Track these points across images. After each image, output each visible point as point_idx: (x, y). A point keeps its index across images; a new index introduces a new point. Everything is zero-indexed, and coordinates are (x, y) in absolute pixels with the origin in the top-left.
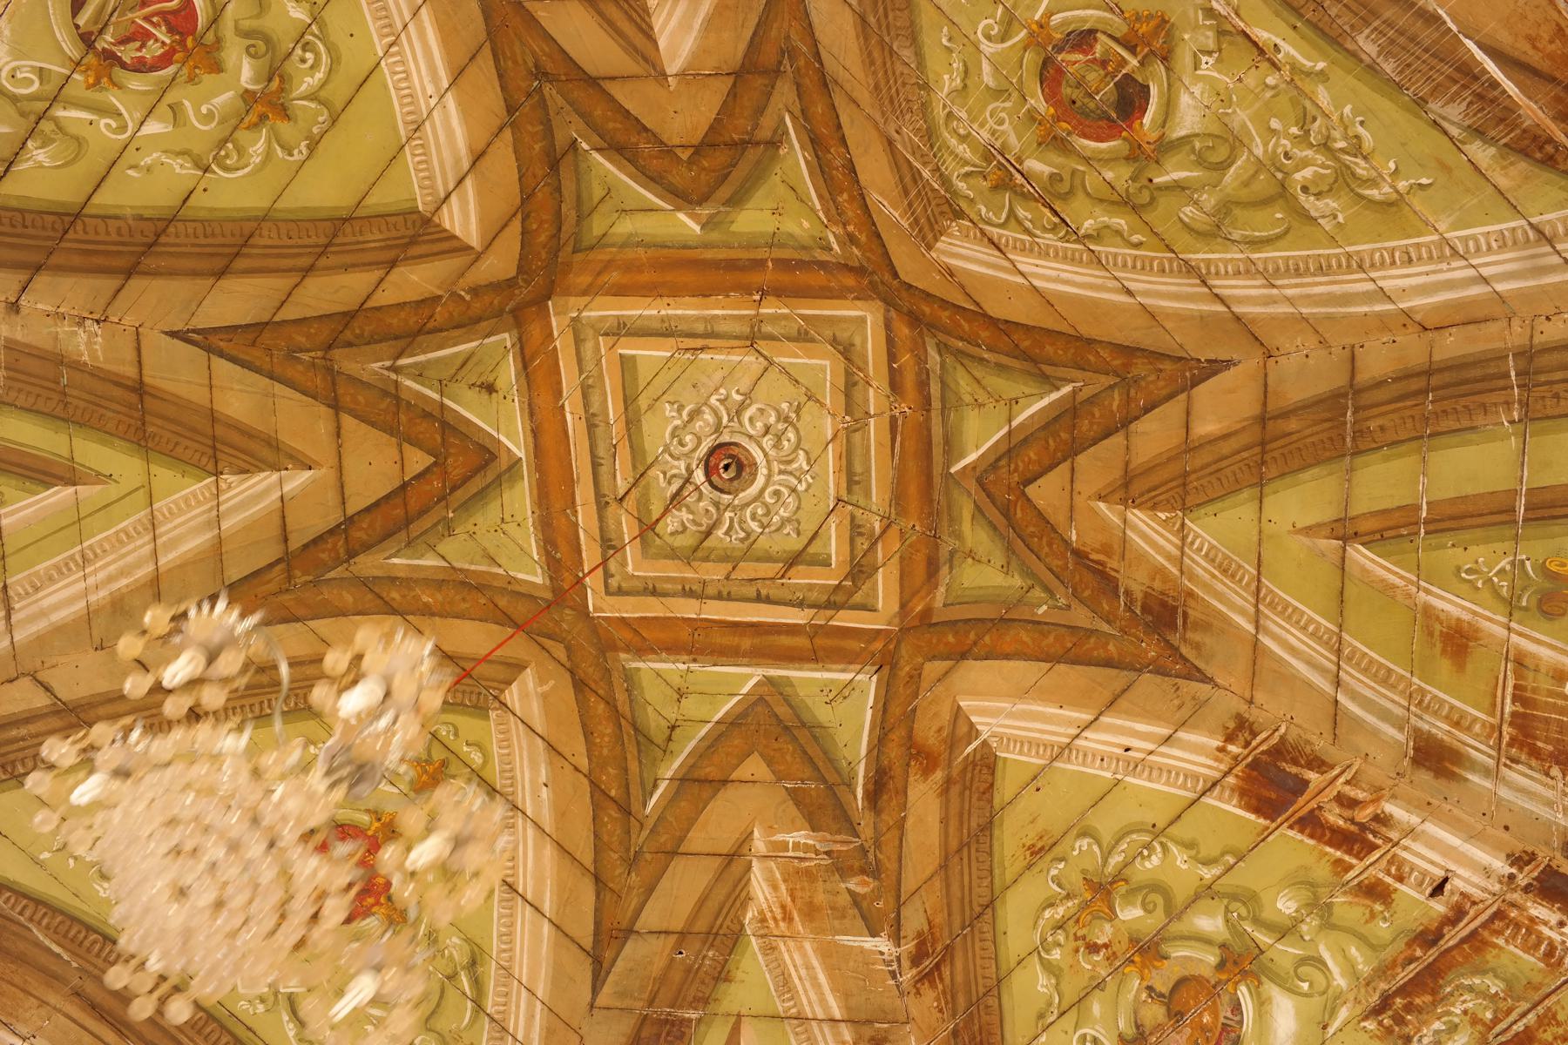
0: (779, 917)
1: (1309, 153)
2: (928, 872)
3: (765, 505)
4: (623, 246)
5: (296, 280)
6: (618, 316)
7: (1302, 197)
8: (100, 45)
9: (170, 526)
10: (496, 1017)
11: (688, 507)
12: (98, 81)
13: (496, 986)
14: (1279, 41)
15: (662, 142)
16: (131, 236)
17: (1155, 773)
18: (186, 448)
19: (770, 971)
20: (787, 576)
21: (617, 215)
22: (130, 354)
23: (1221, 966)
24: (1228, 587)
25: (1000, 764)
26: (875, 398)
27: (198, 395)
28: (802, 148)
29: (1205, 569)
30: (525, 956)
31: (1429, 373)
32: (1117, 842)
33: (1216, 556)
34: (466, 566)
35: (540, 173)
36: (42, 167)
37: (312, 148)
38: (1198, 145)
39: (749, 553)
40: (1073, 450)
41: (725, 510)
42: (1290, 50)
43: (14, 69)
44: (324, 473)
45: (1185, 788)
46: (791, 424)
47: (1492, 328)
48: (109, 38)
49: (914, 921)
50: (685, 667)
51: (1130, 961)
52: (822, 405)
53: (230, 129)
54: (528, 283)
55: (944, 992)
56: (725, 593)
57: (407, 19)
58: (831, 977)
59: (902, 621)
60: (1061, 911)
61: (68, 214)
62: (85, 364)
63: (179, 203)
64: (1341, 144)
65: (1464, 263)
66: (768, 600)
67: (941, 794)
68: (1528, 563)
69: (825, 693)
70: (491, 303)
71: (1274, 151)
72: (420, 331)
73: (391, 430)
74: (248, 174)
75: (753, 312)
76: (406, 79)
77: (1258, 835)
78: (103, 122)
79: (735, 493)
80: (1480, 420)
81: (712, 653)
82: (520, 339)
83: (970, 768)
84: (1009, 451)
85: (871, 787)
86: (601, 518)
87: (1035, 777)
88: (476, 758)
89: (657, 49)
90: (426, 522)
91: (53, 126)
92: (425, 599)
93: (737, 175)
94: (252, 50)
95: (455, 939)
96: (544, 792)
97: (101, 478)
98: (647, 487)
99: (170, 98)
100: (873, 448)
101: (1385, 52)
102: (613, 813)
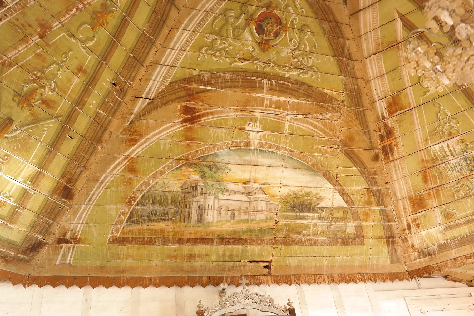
1: (221, 47)
7: (215, 37)
14: (242, 64)
31: (164, 22)
38: (241, 31)
42: (239, 64)
47: (162, 41)
64: (217, 53)
65: (179, 49)
68: (116, 9)
71: (227, 42)
80: (149, 24)
101: (224, 76)
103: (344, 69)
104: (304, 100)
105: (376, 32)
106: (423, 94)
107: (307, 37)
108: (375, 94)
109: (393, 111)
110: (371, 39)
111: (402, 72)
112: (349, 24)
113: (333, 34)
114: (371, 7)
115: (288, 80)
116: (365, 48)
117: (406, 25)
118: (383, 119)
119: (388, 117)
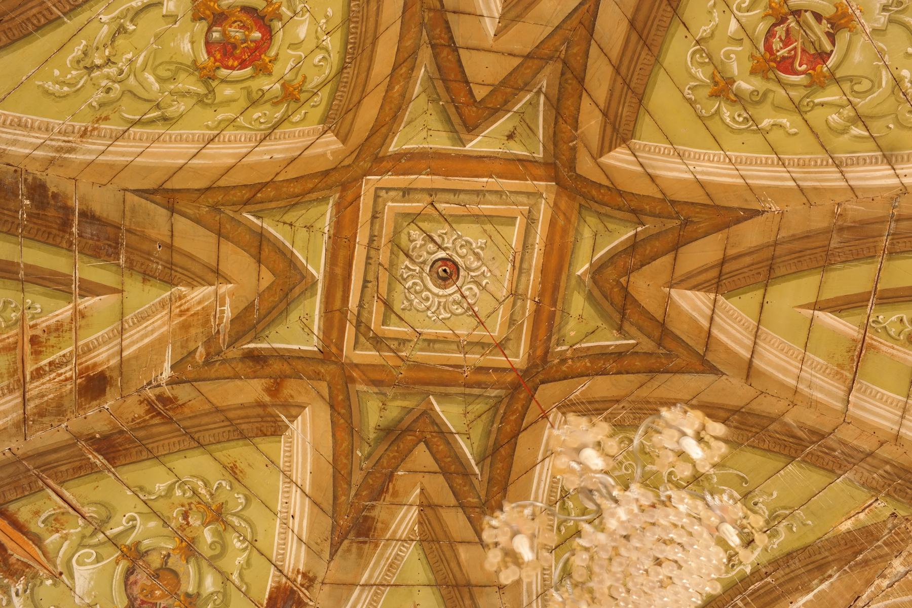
0: (182, 308)
2: (213, 400)
3: (421, 292)
4: (577, 230)
5: (613, 62)
6: (539, 220)
8: (791, 18)
10: (127, 134)
11: (424, 245)
12: (771, 7)
13: (148, 133)
15: (633, 271)
17: (283, 536)
19: (150, 307)
20: (379, 300)
21: (595, 230)
23: (188, 595)
24: (382, 569)
25: (277, 439)
26: (475, 358)
28: (617, 346)
29: (391, 554)
30: (165, 150)
32: (245, 520)
33: (398, 560)
34: (409, 110)
35: (632, 204)
37: (689, 101)
39: (395, 279)
40: (445, 473)
41: (420, 267)
44: (490, 41)
45: (278, 554)
46: (466, 311)
48: (793, 24)
49: (183, 393)
50: (326, 231)
51: (182, 540)
52: (474, 330)
53: (716, 64)
54: (570, 177)
55: (145, 421)
56: (370, 261)
58: (147, 346)
59: (347, 364)
60: (203, 492)
63: (684, 20)
66: (364, 287)
67: (257, 402)
69: (306, 316)
70: (563, 155)
73: (503, 83)
74: (686, 62)
75: (529, 296)
76: (709, 160)
77: (258, 602)
79: (430, 275)
81: (333, 248)
82: (536, 162)
83: (273, 419)
84: (442, 432)
85: (256, 353)
86: (422, 190)
87: (273, 463)
88: (296, 118)
89: (686, 289)
90: (441, 90)
92: (397, 87)
93: (606, 305)
94: (756, 93)
95: (183, 107)
96: (267, 157)
98: (439, 222)
99: (746, 41)
100: (447, 355)
102: (247, 195)
103: (830, 463)
104: (822, 582)
105: (809, 362)
107: (715, 480)
110: (817, 377)
112: (759, 393)
113: (751, 431)
114: (758, 341)
115: (757, 576)
116: (826, 398)
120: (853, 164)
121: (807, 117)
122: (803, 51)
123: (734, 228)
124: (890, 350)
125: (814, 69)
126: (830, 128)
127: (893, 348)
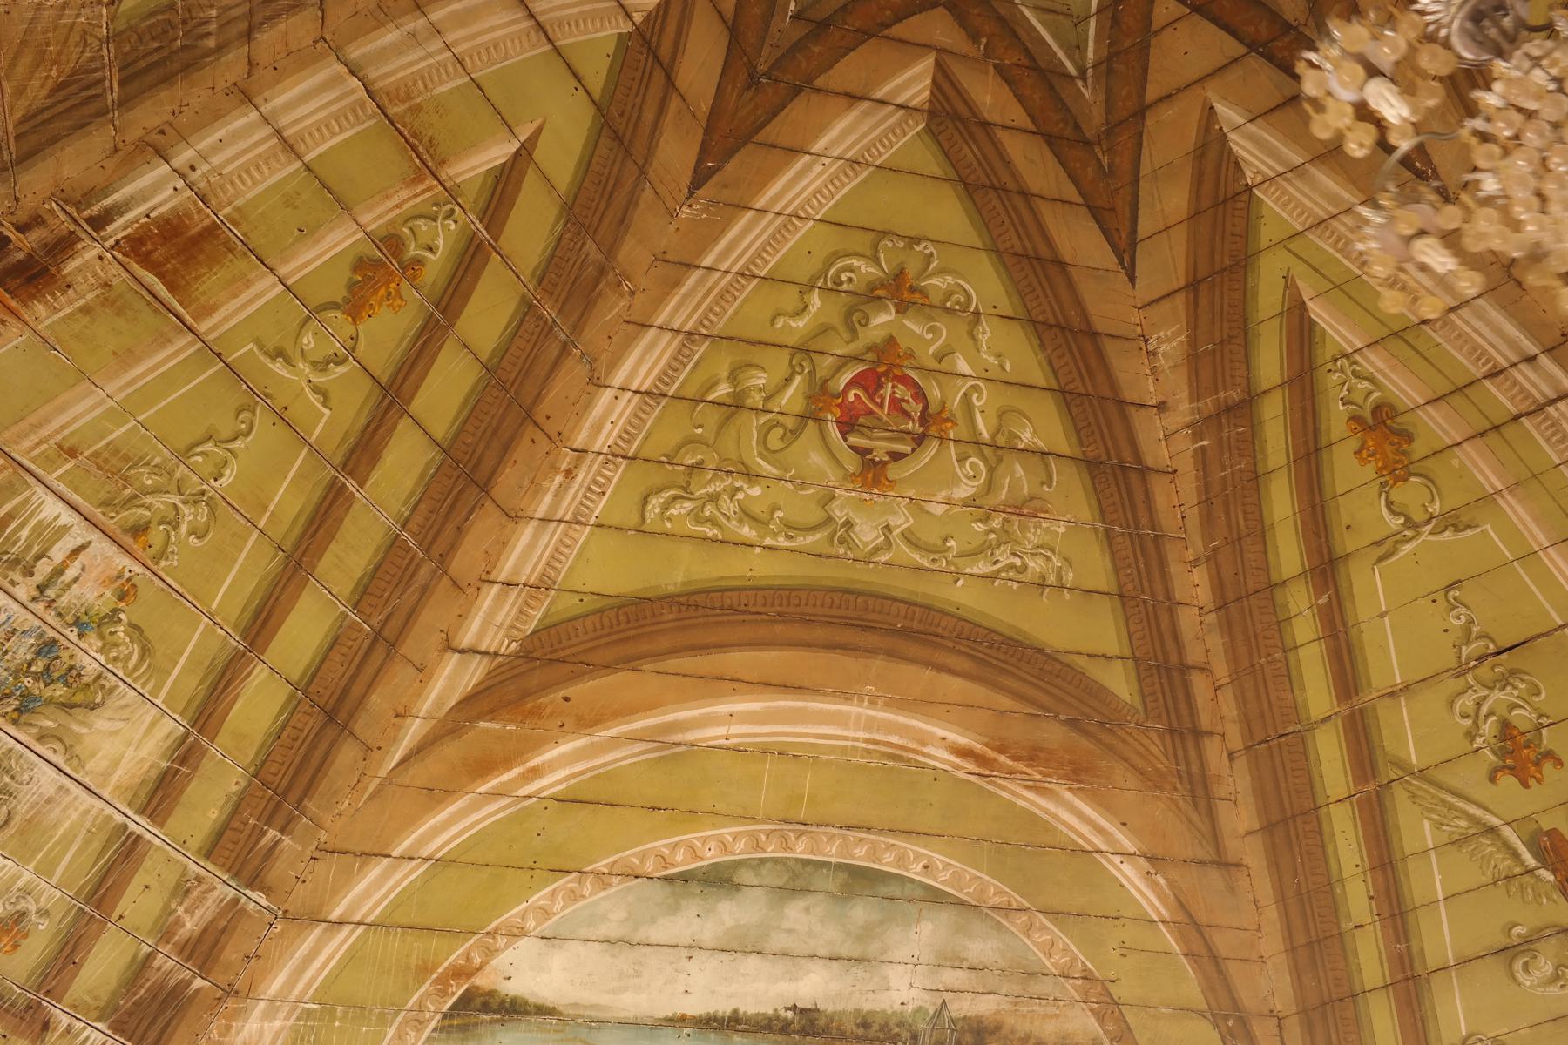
9: (1316, 209)
16: (1061, 346)
18: (1234, 225)
22: (1166, 306)
27: (1180, 236)
36: (1035, 432)
43: (969, 478)
44: (1212, 93)
57: (772, 215)
61: (1065, 399)
62: (1188, 336)
63: (1015, 324)
70: (979, 15)
72: (1035, 67)
73: (1144, 50)
76: (820, 192)
78: (977, 404)
91: (999, 436)
94: (863, 322)
97: (1289, 283)
99: (933, 365)
106: (270, 346)
108: (199, 147)
109: (150, 253)
111: (332, 229)
114: (532, 22)
116: (379, 43)
117: (504, 179)
118: (89, 220)
119: (112, 241)
120: (679, 352)
121: (786, 352)
122: (871, 412)
123: (699, 137)
124: (396, 200)
125: (839, 406)
126: (751, 365)
127: (397, 206)
